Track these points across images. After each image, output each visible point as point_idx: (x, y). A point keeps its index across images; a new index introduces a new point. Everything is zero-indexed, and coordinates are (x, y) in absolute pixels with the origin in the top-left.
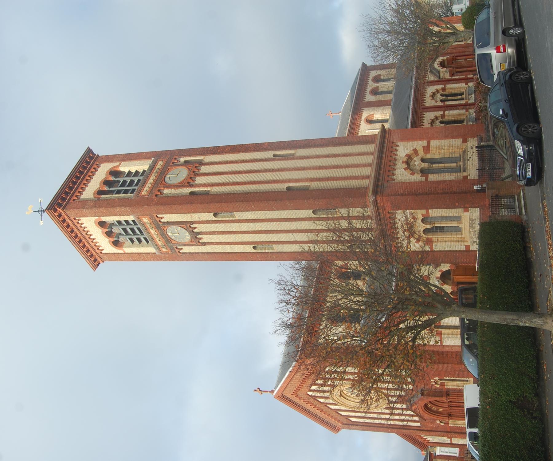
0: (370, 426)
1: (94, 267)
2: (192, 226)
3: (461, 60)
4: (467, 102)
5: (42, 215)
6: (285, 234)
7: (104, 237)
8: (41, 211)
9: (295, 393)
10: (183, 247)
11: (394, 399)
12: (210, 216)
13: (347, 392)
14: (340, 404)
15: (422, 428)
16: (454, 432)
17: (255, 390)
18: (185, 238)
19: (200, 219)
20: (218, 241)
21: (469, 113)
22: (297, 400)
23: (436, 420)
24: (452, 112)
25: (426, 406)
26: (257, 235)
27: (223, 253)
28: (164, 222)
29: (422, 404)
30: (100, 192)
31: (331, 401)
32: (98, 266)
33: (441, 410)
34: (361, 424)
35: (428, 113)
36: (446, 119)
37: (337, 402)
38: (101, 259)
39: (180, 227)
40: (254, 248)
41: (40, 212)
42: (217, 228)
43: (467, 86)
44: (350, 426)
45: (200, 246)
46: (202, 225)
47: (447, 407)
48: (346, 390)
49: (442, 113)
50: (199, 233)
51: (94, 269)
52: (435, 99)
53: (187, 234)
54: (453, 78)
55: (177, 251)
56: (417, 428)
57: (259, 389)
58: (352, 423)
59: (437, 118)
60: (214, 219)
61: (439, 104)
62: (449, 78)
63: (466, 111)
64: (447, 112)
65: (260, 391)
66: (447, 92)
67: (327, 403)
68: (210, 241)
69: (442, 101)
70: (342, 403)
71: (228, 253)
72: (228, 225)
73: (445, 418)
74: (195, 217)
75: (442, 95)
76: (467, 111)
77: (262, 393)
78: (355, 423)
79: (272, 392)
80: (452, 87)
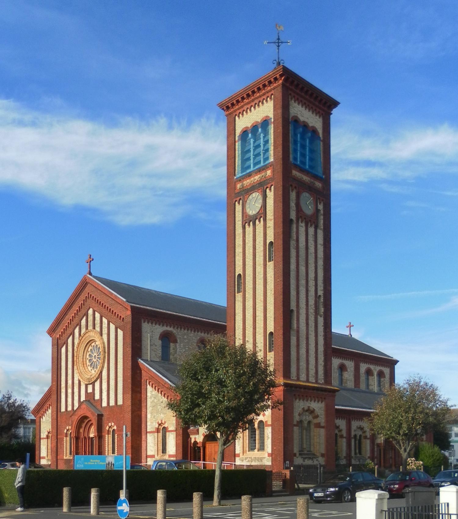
0: (57, 365)
2: (262, 219)
12: (270, 238)
18: (250, 210)
31: (83, 330)
34: (59, 357)
39: (261, 208)
53: (254, 213)
55: (238, 199)
74: (270, 224)
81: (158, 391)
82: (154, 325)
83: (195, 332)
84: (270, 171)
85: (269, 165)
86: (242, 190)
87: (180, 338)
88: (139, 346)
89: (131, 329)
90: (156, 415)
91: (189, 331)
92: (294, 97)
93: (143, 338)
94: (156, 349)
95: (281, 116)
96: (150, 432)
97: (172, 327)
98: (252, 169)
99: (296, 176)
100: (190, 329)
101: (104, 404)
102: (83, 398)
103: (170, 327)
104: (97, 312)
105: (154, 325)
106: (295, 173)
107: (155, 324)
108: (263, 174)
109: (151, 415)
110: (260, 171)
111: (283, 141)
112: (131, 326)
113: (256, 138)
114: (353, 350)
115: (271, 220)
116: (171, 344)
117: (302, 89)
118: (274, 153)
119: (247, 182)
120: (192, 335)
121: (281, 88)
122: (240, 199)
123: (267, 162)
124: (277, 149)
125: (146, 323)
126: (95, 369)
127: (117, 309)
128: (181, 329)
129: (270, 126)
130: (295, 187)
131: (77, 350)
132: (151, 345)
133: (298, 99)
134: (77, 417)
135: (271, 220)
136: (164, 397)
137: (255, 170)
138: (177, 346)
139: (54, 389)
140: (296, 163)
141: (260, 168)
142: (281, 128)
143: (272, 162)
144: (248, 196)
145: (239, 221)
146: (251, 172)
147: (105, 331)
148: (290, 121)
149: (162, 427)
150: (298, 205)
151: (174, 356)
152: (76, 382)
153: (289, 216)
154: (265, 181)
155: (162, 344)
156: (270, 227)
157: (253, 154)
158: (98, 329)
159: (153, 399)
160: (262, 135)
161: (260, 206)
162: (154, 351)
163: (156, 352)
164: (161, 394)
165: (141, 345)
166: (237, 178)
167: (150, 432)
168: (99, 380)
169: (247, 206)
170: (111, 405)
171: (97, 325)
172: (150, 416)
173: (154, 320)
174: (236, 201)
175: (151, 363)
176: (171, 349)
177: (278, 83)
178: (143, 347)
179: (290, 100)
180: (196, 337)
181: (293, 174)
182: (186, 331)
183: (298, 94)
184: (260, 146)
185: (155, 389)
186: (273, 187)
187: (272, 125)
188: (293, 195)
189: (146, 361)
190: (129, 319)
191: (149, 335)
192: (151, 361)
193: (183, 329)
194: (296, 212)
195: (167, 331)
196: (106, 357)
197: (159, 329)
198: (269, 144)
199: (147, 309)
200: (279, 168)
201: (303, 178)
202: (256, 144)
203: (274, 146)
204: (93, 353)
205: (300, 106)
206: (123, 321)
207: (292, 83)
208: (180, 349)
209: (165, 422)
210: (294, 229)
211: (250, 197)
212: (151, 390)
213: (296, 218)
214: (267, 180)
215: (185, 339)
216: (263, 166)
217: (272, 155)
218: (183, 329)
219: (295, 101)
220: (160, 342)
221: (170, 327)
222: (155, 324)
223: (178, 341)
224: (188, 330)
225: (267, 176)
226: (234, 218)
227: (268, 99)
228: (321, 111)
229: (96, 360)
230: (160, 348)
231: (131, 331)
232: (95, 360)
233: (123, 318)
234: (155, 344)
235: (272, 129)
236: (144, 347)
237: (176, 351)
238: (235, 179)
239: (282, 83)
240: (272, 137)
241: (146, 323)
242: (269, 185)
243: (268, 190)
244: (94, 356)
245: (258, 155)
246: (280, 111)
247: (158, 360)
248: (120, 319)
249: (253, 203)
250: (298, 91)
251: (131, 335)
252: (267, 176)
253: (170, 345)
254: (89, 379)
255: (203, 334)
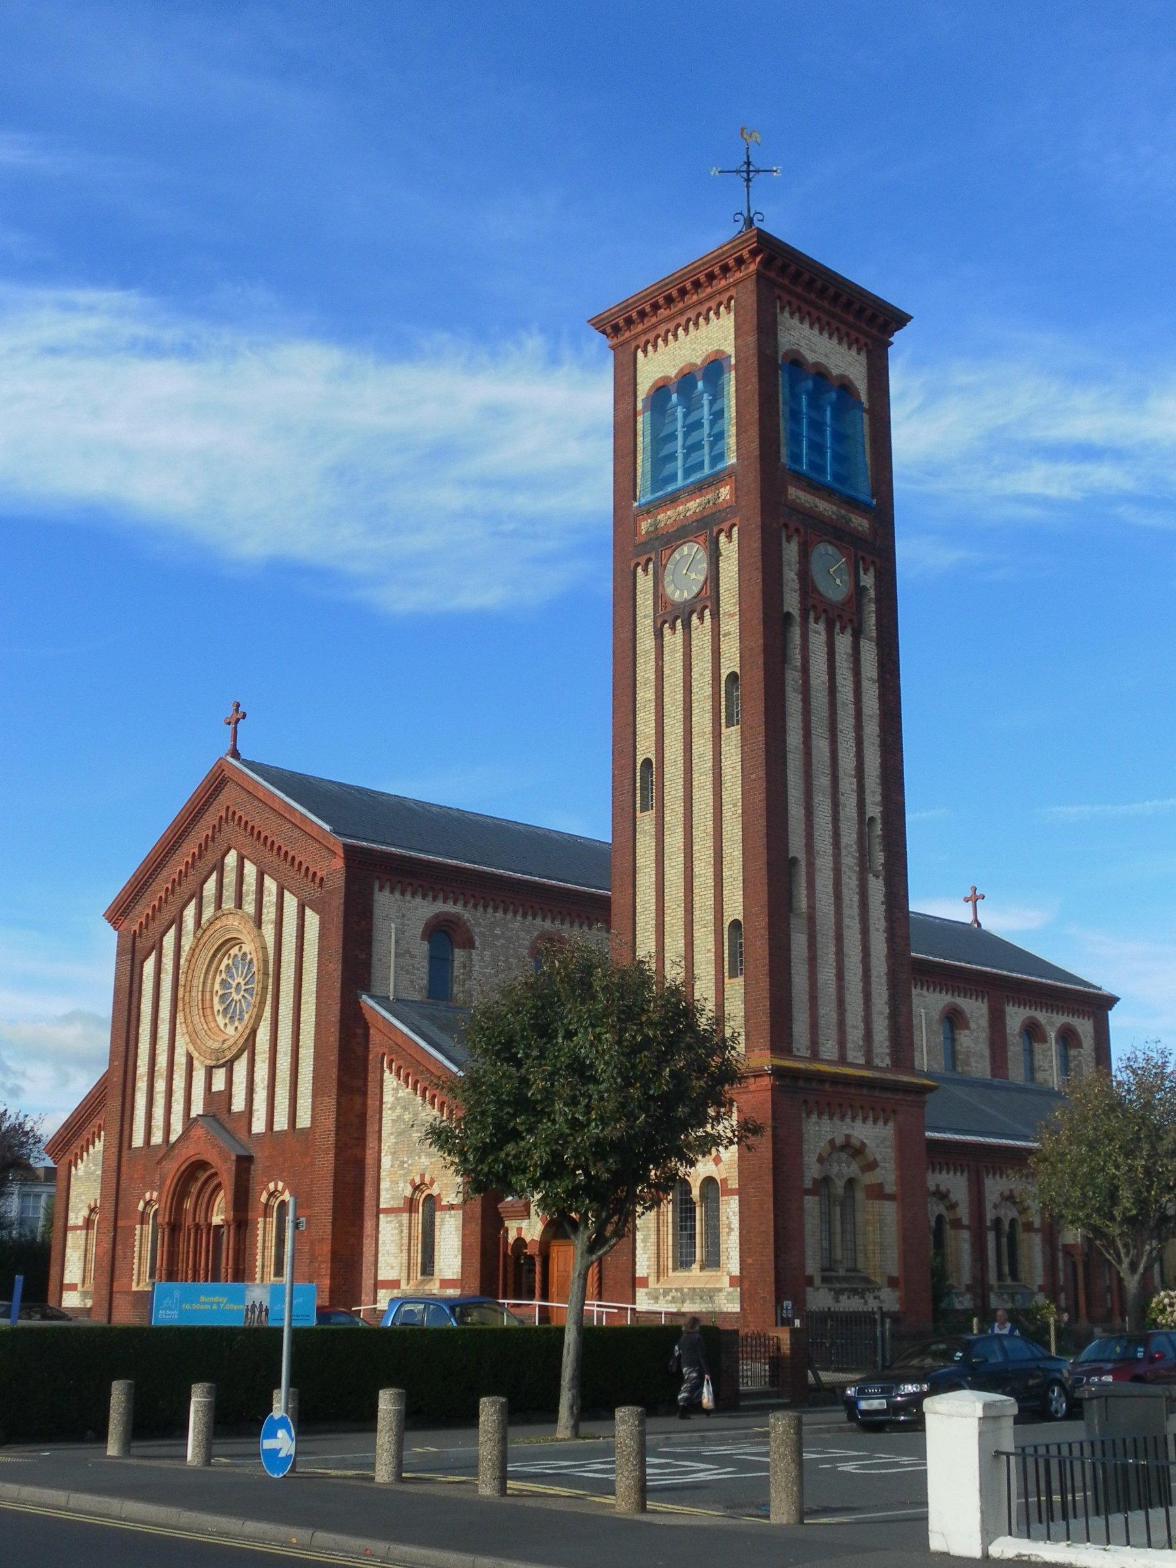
1: (599, 321)
2: (707, 612)
3: (1107, 1276)
4: (991, 1288)
5: (738, 172)
6: (682, 844)
7: (681, 366)
8: (748, 172)
9: (230, 816)
10: (650, 576)
11: (219, 1084)
13: (236, 956)
14: (201, 937)
15: (125, 1152)
16: (115, 1237)
17: (238, 705)
18: (677, 588)
19: (726, 635)
20: (666, 671)
21: (962, 1294)
22: (210, 818)
23: (160, 1189)
24: (966, 1247)
25: (202, 1165)
26: (681, 773)
27: (635, 680)
28: (717, 542)
29: (212, 1157)
30: (796, 362)
31: (208, 912)
32: (601, 332)
33: (188, 1204)
35: (966, 1183)
36: (949, 1232)
37: (207, 929)
38: (622, 344)
39: (705, 582)
40: (647, 762)
41: (745, 168)
42: (701, 674)
43: (1036, 1289)
44: (129, 957)
45: (655, 622)
46: (709, 637)
47: (194, 1219)
48: (240, 955)
49: (965, 1221)
50: (687, 626)
51: (594, 321)
52: (1003, 1203)
53: (686, 596)
54: (1060, 1254)
55: (643, 560)
56: (126, 1139)
57: (244, 717)
58: (137, 962)
59: (953, 1207)
60: (725, 673)
61: (990, 1215)
62: (1060, 1244)
63: (967, 1286)
64: (966, 1234)
65: (237, 721)
66: (1022, 1236)
67: (201, 898)
68: (666, 650)
69: (998, 1222)
70: (202, 941)
71: (635, 693)
72: (708, 705)
73: (167, 1214)
75: (1013, 1222)
76: (969, 1288)
77: (229, 724)
78: (137, 971)
79: (235, 754)
80: (1033, 1251)
81: (415, 1089)
82: (408, 898)
83: (524, 916)
84: (728, 487)
85: (727, 472)
86: (652, 535)
87: (481, 933)
88: (363, 956)
89: (342, 908)
90: (405, 1159)
91: (509, 916)
92: (790, 303)
93: (378, 936)
94: (413, 965)
95: (755, 351)
96: (388, 1211)
97: (461, 903)
98: (680, 483)
99: (798, 501)
100: (511, 907)
101: (258, 1126)
102: (197, 1109)
103: (455, 904)
104: (248, 858)
105: (408, 898)
106: (795, 494)
107: (413, 896)
108: (709, 496)
109: (392, 1160)
110: (700, 489)
111: (761, 411)
112: (342, 901)
113: (691, 404)
114: (984, 969)
115: (732, 615)
116: (456, 951)
117: (811, 283)
118: (738, 443)
119: (667, 517)
120: (517, 925)
121: (754, 281)
122: (649, 560)
123: (719, 467)
124: (746, 432)
125: (386, 892)
126: (236, 1024)
127: (307, 855)
128: (485, 907)
129: (726, 375)
130: (797, 530)
131: (189, 968)
132: (397, 955)
133: (799, 309)
134: (176, 1165)
135: (732, 615)
136: (429, 1107)
137: (688, 486)
138: (474, 956)
139: (117, 1079)
140: (797, 467)
141: (700, 481)
142: (755, 380)
143: (732, 465)
144: (668, 552)
145: (645, 617)
146: (679, 490)
147: (269, 913)
148: (780, 362)
149: (423, 1196)
150: (805, 576)
151: (463, 985)
152: (180, 1059)
153: (782, 605)
154: (715, 513)
155: (431, 949)
156: (729, 634)
157: (684, 445)
158: (249, 907)
159: (399, 1111)
160: (706, 398)
161: (702, 578)
162: (408, 972)
163: (413, 974)
164: (424, 1096)
165: (370, 955)
166: (640, 506)
167: (388, 1211)
168: (245, 1055)
169: (668, 579)
170: (277, 1128)
171: (248, 895)
172: (390, 1163)
173: (410, 884)
174: (638, 564)
175: (398, 1006)
176: (456, 964)
177: (745, 269)
178: (375, 959)
179: (778, 310)
180: (528, 932)
181: (789, 497)
182: (499, 915)
183: (799, 297)
184: (702, 425)
185: (407, 1082)
186: (735, 529)
187: (733, 373)
188: (791, 551)
189: (383, 1000)
190: (339, 881)
191: (393, 925)
192: (398, 1000)
193: (490, 910)
194: (800, 596)
195: (446, 913)
196: (270, 987)
197: (424, 909)
198: (726, 420)
199: (390, 854)
200: (752, 481)
201: (816, 506)
202: (690, 420)
203: (737, 424)
204: (232, 977)
205: (806, 326)
206: (321, 886)
207: (783, 269)
208: (481, 967)
209: (432, 1182)
210: (797, 640)
211: (676, 555)
212: (395, 1083)
213: (800, 610)
214: (720, 511)
215: (497, 937)
216: (711, 476)
217: (734, 448)
218: (490, 910)
219: (792, 314)
220: (425, 946)
221: (455, 904)
222: (413, 896)
223: (477, 944)
224: (505, 912)
225: (721, 500)
226: (631, 609)
227: (722, 308)
228: (861, 337)
229: (240, 997)
230: (425, 963)
231: (341, 914)
232: (237, 997)
233: (322, 879)
234: (410, 953)
235: (733, 382)
236: (380, 960)
237: (471, 971)
238: (636, 507)
239: (757, 270)
240: (733, 402)
241: (386, 892)
242: (726, 526)
243: (722, 538)
244: (234, 985)
245: (698, 446)
246: (752, 339)
247: (417, 997)
248: (313, 881)
249: (685, 571)
250: (799, 290)
251: (341, 925)
252: (721, 500)
253: (453, 955)
254: (216, 1051)
255: (548, 924)
